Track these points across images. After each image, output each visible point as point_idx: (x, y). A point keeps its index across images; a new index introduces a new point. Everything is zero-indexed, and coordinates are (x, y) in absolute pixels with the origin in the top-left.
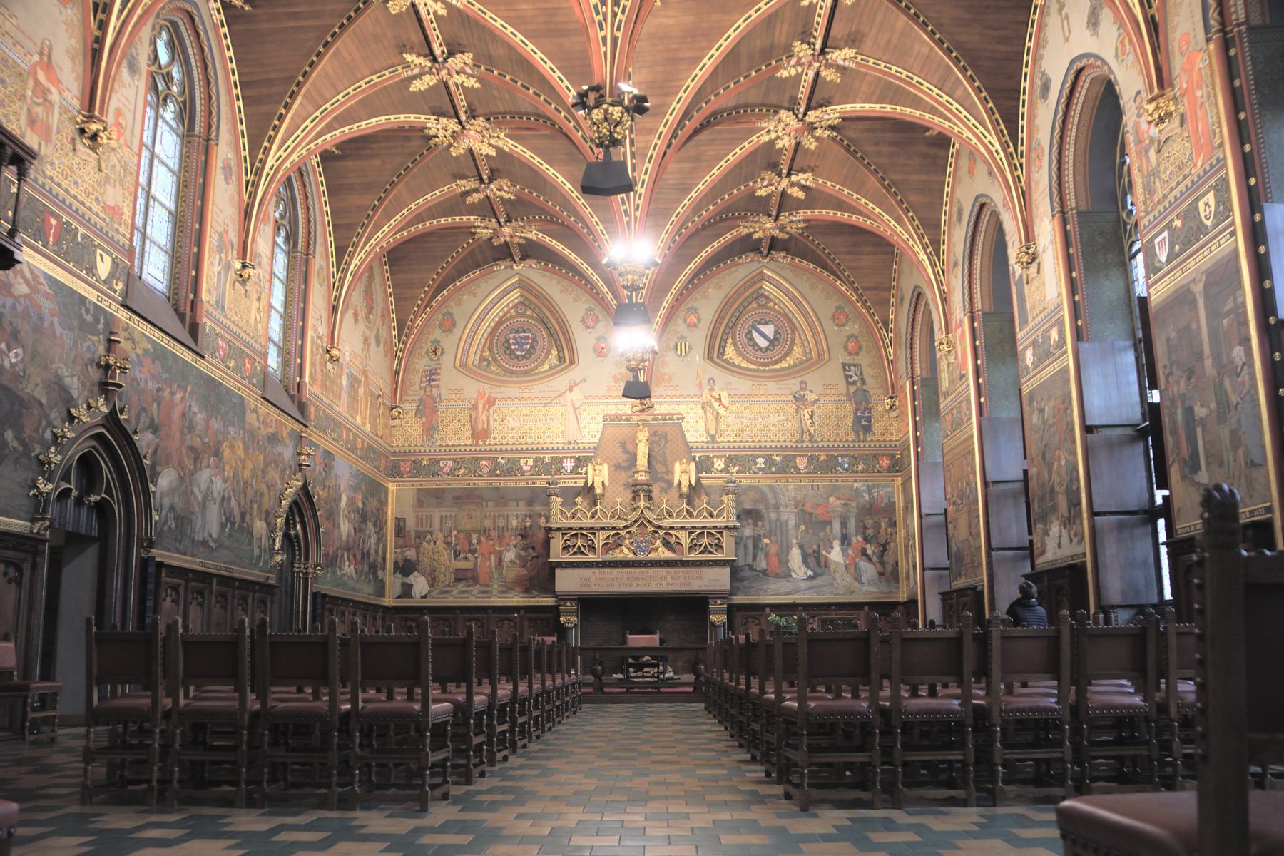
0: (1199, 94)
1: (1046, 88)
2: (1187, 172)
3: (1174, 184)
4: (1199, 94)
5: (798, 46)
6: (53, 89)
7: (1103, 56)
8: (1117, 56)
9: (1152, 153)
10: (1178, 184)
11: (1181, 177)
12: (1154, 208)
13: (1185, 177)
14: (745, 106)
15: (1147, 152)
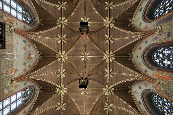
0: (161, 75)
1: (140, 103)
2: (170, 83)
3: (170, 87)
4: (161, 75)
5: (106, 104)
6: (13, 73)
7: (144, 89)
8: (146, 87)
9: (162, 89)
10: (171, 86)
11: (170, 85)
12: (171, 95)
13: (171, 84)
14: (103, 28)
15: (161, 90)
